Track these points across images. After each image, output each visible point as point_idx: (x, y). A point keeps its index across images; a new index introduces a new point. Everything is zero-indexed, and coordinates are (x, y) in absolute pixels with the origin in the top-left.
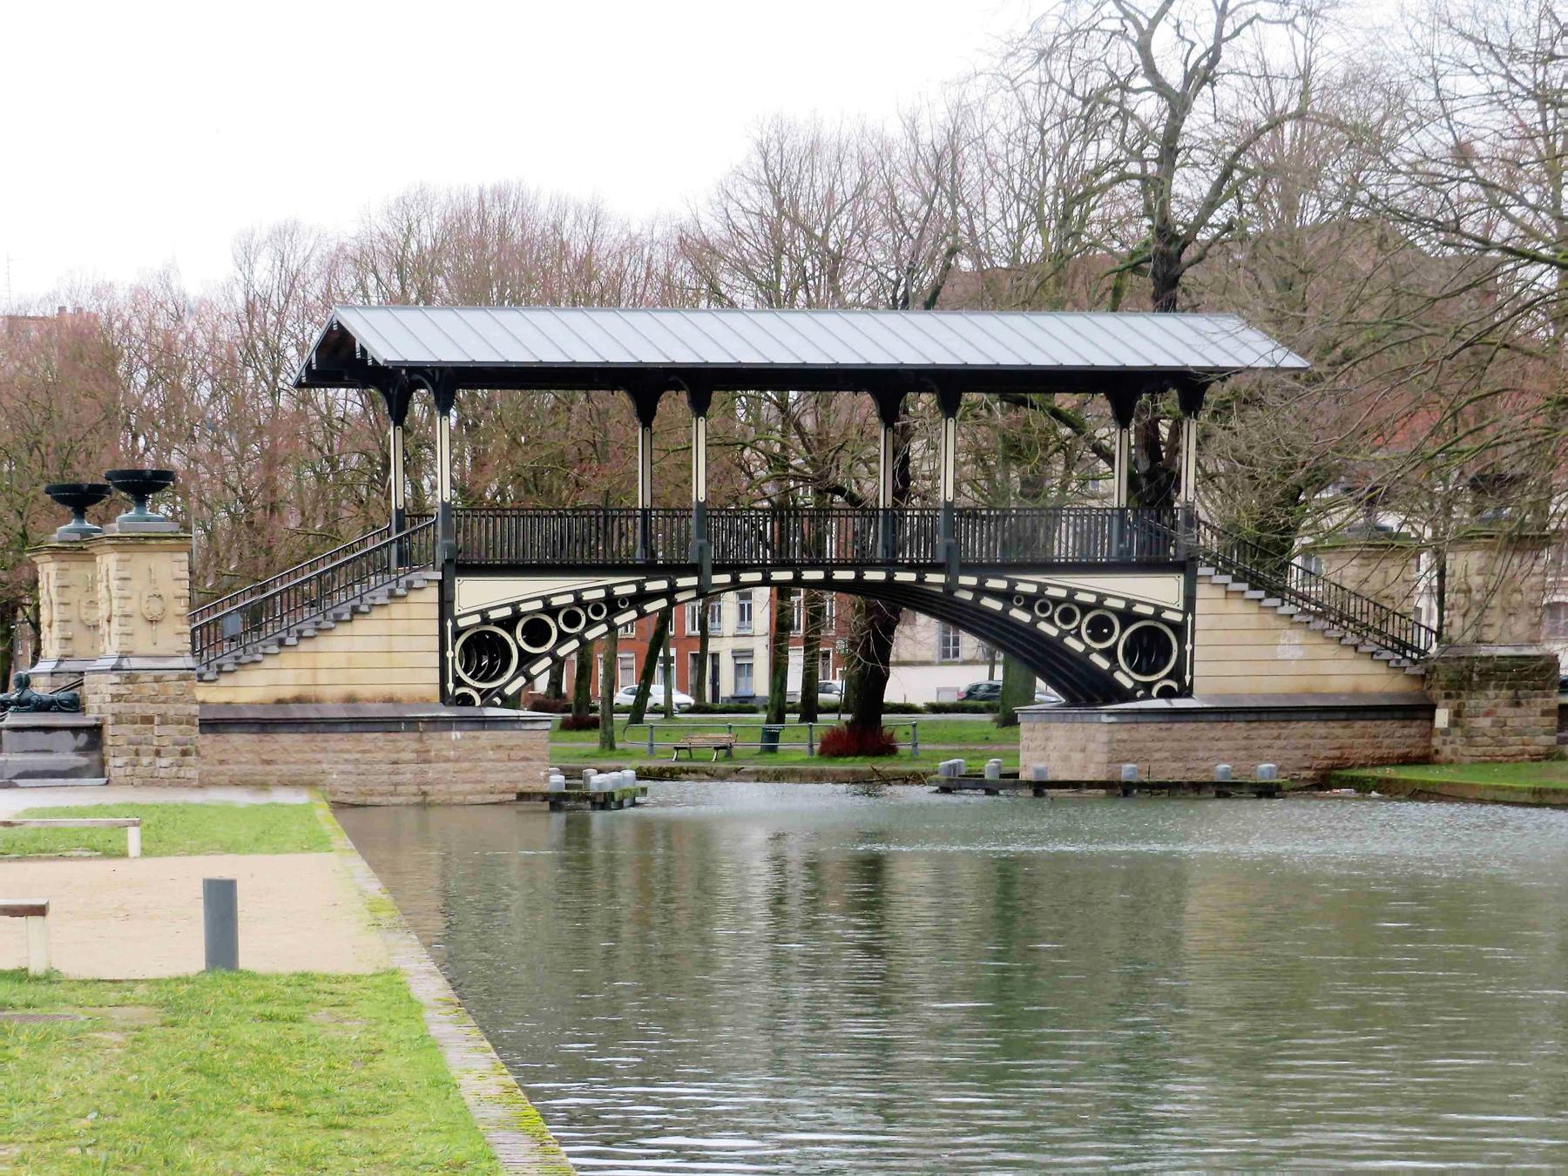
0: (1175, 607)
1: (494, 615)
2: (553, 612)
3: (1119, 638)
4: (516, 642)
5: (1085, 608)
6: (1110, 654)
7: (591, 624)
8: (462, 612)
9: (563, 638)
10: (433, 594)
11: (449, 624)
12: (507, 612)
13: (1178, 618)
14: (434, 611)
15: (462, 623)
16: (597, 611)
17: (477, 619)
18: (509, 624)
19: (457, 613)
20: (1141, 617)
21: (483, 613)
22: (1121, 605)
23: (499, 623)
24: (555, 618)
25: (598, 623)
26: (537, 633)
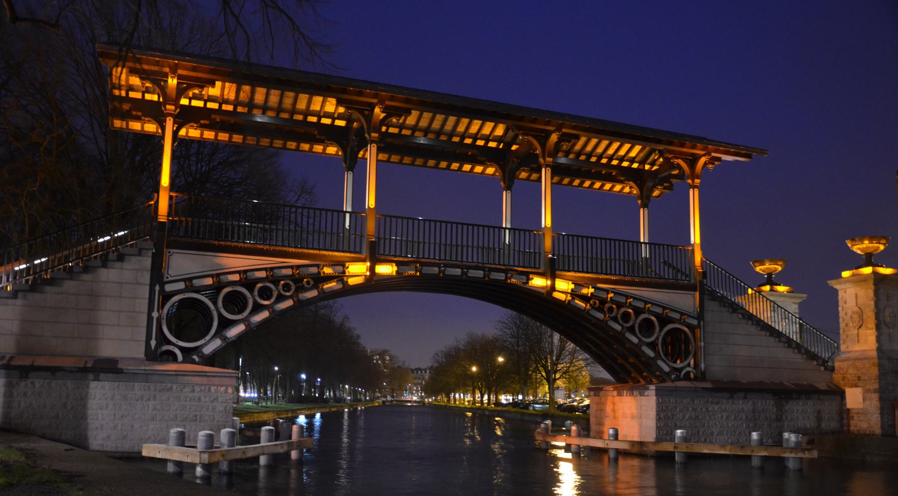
0: (692, 315)
1: (197, 283)
2: (249, 284)
3: (658, 335)
4: (217, 309)
5: (638, 311)
6: (652, 346)
7: (281, 298)
8: (170, 279)
9: (257, 308)
10: (147, 262)
11: (157, 288)
12: (209, 281)
13: (695, 322)
14: (146, 278)
15: (169, 288)
16: (287, 287)
17: (181, 286)
19: (165, 280)
20: (671, 321)
21: (188, 280)
22: (659, 310)
24: (251, 290)
26: (235, 302)
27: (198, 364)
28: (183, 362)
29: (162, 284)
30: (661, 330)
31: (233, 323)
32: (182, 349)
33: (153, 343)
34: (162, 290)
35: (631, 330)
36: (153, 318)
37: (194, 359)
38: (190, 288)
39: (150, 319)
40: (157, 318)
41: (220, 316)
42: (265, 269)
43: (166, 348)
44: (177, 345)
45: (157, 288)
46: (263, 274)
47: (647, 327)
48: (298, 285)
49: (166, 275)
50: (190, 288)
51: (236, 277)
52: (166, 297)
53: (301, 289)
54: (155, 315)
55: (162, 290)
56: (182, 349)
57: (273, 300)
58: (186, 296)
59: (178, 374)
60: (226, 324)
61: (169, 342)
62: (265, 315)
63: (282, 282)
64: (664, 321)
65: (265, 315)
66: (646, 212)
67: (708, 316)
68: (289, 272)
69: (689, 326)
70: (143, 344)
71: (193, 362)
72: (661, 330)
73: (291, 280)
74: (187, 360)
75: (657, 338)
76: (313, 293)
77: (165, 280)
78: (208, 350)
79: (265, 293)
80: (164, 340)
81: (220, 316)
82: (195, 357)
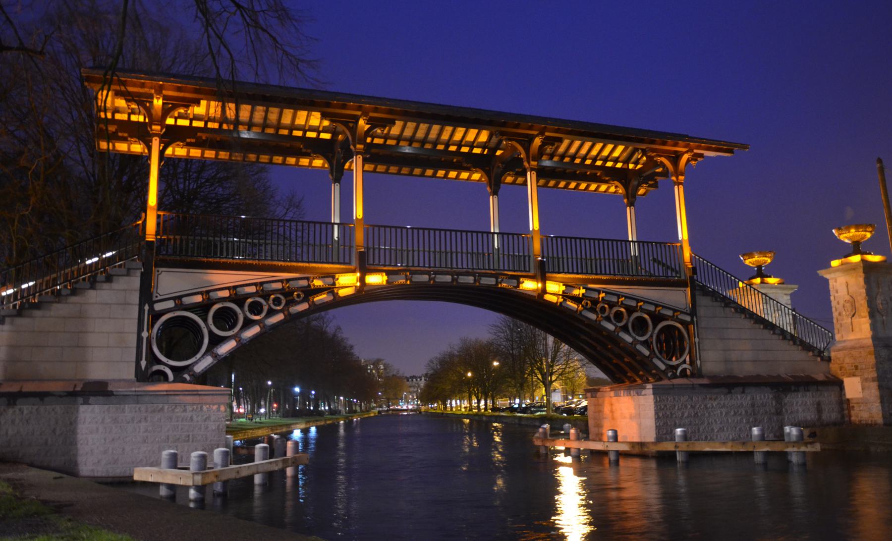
0: (685, 311)
1: (187, 301)
2: (239, 300)
3: (653, 332)
4: (207, 326)
5: (630, 310)
6: (646, 343)
7: (271, 313)
8: (159, 298)
9: (248, 324)
10: (135, 282)
11: (147, 307)
12: (198, 299)
13: (688, 318)
14: (135, 298)
15: (158, 307)
16: (277, 301)
17: (171, 304)
18: (202, 309)
19: (155, 299)
20: (664, 318)
21: (178, 299)
22: (652, 308)
23: (192, 308)
24: (241, 306)
25: (277, 312)
26: (225, 318)
27: (190, 382)
28: (174, 382)
29: (152, 304)
30: (654, 328)
31: (223, 340)
32: (173, 368)
33: (143, 363)
34: (151, 308)
35: (625, 329)
36: (143, 338)
37: (185, 379)
38: (180, 306)
39: (140, 339)
40: (147, 338)
41: (211, 333)
42: (255, 284)
43: (156, 368)
44: (167, 364)
45: (147, 307)
46: (252, 289)
47: (640, 326)
48: (288, 299)
49: (155, 294)
50: (180, 306)
51: (226, 294)
52: (156, 316)
53: (291, 302)
54: (145, 334)
55: (151, 308)
56: (173, 368)
57: (263, 315)
58: (176, 315)
59: (169, 394)
60: (216, 341)
61: (159, 362)
62: (255, 330)
63: (272, 297)
64: (657, 318)
65: (255, 330)
66: (633, 211)
67: (701, 311)
68: (278, 286)
69: (682, 322)
70: (134, 365)
71: (184, 381)
72: (654, 328)
73: (281, 294)
74: (179, 379)
75: (651, 336)
76: (304, 306)
77: (155, 299)
78: (199, 368)
79: (256, 308)
80: (154, 360)
81: (211, 333)
82: (187, 376)
